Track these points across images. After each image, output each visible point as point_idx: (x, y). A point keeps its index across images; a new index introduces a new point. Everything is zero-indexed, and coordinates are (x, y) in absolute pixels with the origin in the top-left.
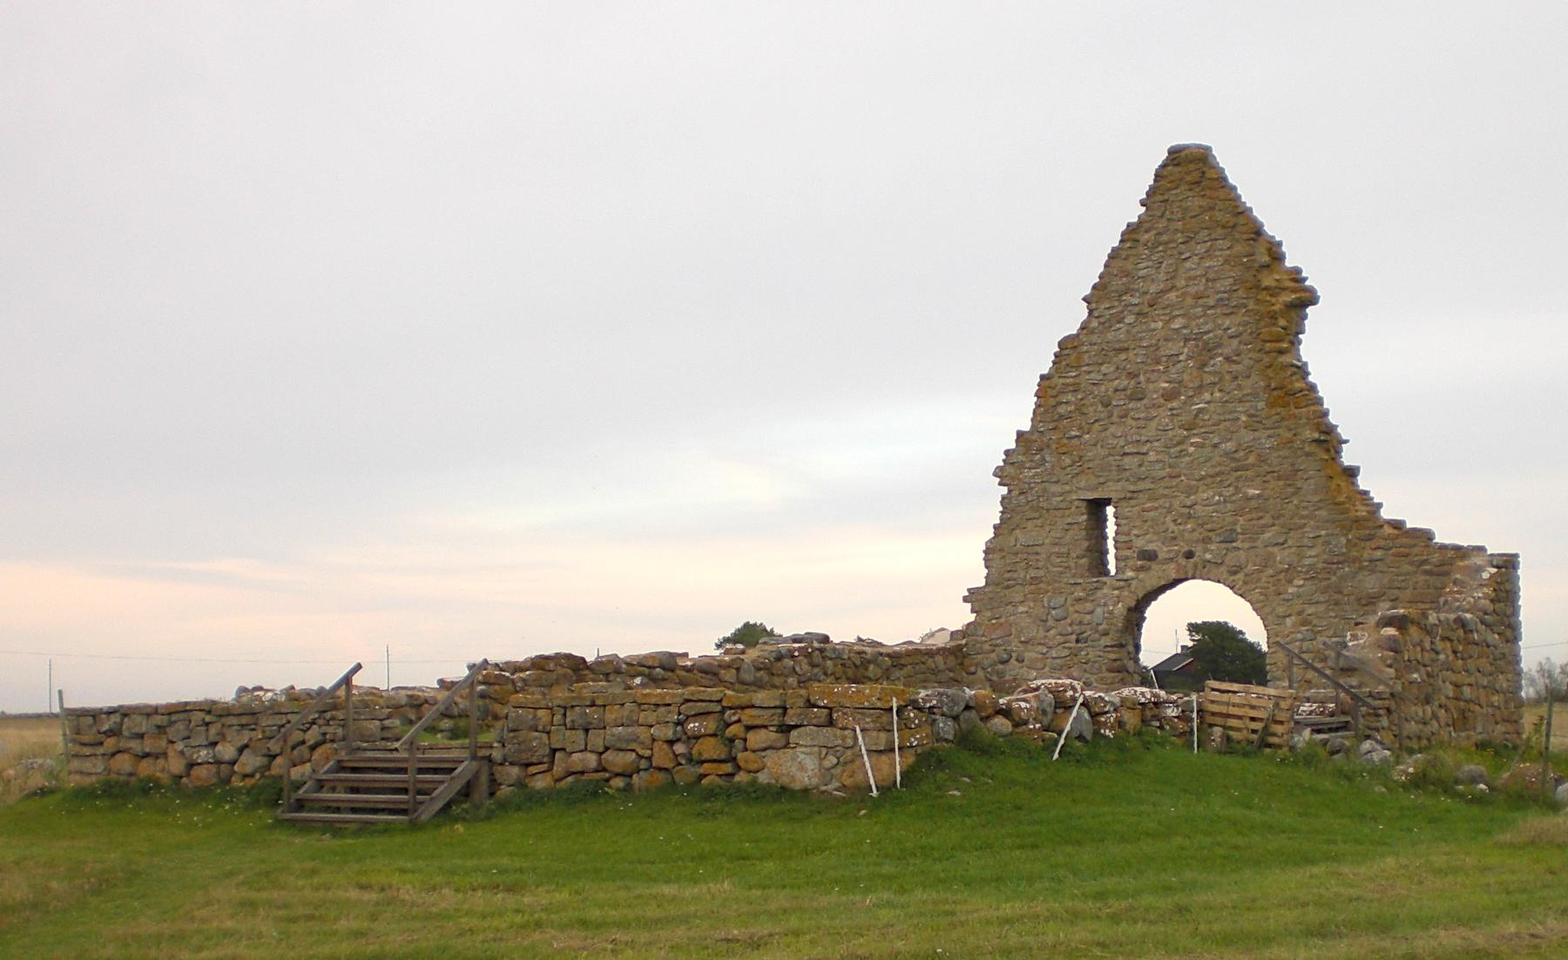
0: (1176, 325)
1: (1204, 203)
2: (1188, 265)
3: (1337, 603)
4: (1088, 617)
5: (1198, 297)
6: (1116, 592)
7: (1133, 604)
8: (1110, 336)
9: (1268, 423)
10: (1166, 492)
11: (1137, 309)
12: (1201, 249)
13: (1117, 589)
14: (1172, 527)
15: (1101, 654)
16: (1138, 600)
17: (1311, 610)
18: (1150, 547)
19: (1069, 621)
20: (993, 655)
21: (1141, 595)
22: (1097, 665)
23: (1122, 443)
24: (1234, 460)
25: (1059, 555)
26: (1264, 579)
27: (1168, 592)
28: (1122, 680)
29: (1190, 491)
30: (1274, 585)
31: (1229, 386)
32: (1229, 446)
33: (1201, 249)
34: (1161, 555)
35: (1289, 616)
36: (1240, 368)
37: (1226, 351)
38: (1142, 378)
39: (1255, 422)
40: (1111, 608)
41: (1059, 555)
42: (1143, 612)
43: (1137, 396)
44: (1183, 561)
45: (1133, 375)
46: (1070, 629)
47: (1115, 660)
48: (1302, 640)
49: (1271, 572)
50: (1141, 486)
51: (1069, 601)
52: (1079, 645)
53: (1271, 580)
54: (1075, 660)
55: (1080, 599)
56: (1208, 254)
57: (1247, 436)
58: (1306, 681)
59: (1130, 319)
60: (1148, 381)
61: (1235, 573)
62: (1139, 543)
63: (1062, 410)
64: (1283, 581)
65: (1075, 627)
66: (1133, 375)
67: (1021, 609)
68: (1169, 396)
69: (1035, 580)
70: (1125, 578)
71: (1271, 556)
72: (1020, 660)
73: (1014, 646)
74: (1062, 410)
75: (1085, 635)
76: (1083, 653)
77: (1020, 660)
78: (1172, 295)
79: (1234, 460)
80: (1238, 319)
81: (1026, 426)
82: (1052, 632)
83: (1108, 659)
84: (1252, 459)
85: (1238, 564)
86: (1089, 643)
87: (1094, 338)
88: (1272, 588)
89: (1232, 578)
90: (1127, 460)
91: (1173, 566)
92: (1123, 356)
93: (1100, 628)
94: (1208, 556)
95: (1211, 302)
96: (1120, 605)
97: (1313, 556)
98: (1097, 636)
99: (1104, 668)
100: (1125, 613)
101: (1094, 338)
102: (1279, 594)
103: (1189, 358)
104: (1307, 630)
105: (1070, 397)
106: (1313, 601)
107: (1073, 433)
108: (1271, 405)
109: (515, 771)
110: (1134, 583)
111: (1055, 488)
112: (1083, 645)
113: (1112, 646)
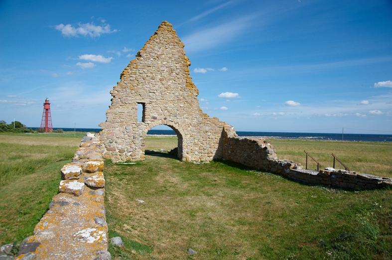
0: (164, 63)
1: (172, 36)
2: (167, 50)
3: (199, 132)
8: (146, 62)
9: (186, 90)
10: (161, 103)
11: (154, 57)
12: (171, 47)
18: (155, 116)
20: (108, 141)
23: (149, 89)
24: (178, 97)
25: (129, 116)
29: (167, 103)
31: (177, 80)
32: (177, 94)
37: (177, 72)
38: (154, 74)
39: (183, 89)
41: (129, 116)
44: (164, 120)
50: (153, 101)
51: (131, 128)
57: (181, 93)
60: (156, 75)
62: (152, 115)
63: (131, 78)
69: (121, 122)
71: (185, 121)
73: (115, 138)
74: (131, 78)
78: (163, 56)
79: (178, 97)
82: (126, 135)
87: (141, 62)
90: (151, 94)
91: (161, 121)
92: (149, 68)
94: (170, 119)
97: (195, 122)
101: (141, 62)
103: (167, 71)
107: (135, 85)
108: (187, 86)
110: (150, 124)
111: (129, 98)
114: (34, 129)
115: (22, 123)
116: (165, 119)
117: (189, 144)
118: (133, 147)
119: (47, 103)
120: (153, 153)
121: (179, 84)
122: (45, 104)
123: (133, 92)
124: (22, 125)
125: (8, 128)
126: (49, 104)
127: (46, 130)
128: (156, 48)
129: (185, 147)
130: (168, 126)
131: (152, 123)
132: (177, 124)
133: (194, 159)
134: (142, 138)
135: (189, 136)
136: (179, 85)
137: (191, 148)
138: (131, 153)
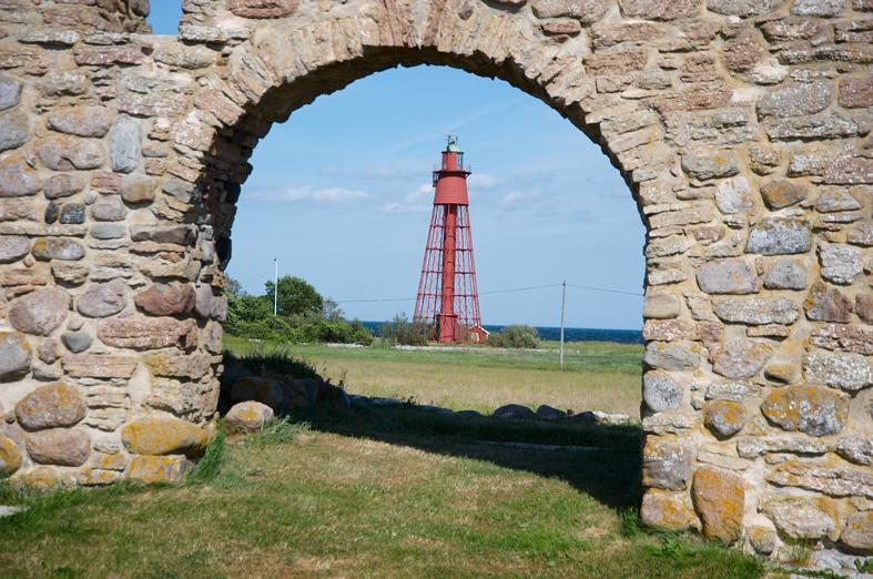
4: (92, 145)
6: (184, 78)
7: (233, 114)
13: (188, 67)
15: (129, 259)
16: (248, 105)
17: (813, 155)
19: (27, 152)
21: (259, 89)
22: (107, 290)
26: (654, 58)
27: (322, 100)
28: (182, 339)
30: (684, 79)
35: (733, 173)
40: (163, 123)
42: (248, 151)
46: (29, 180)
47: (165, 280)
48: (767, 250)
49: (677, 35)
51: (30, 96)
52: (56, 228)
53: (678, 60)
54: (42, 270)
55: (67, 92)
58: (770, 377)
61: (560, 38)
64: (719, 68)
65: (44, 174)
70: (212, 37)
75: (76, 199)
76: (66, 253)
83: (146, 273)
85: (577, 10)
86: (89, 223)
88: (679, 87)
89: (551, 51)
93: (126, 181)
96: (193, 116)
98: (116, 202)
99: (130, 296)
100: (208, 141)
102: (703, 106)
104: (788, 221)
106: (818, 131)
110: (238, 52)
112: (66, 229)
113: (158, 238)
114: (376, 328)
115: (322, 290)
117: (745, 308)
118: (40, 313)
119: (450, 173)
120: (535, 435)
122: (442, 174)
124: (318, 301)
125: (245, 317)
126: (463, 174)
127: (446, 330)
129: (682, 349)
130: (556, 104)
131: (264, 31)
132: (578, 45)
133: (814, 520)
134: (142, 220)
137: (780, 358)
138: (27, 386)
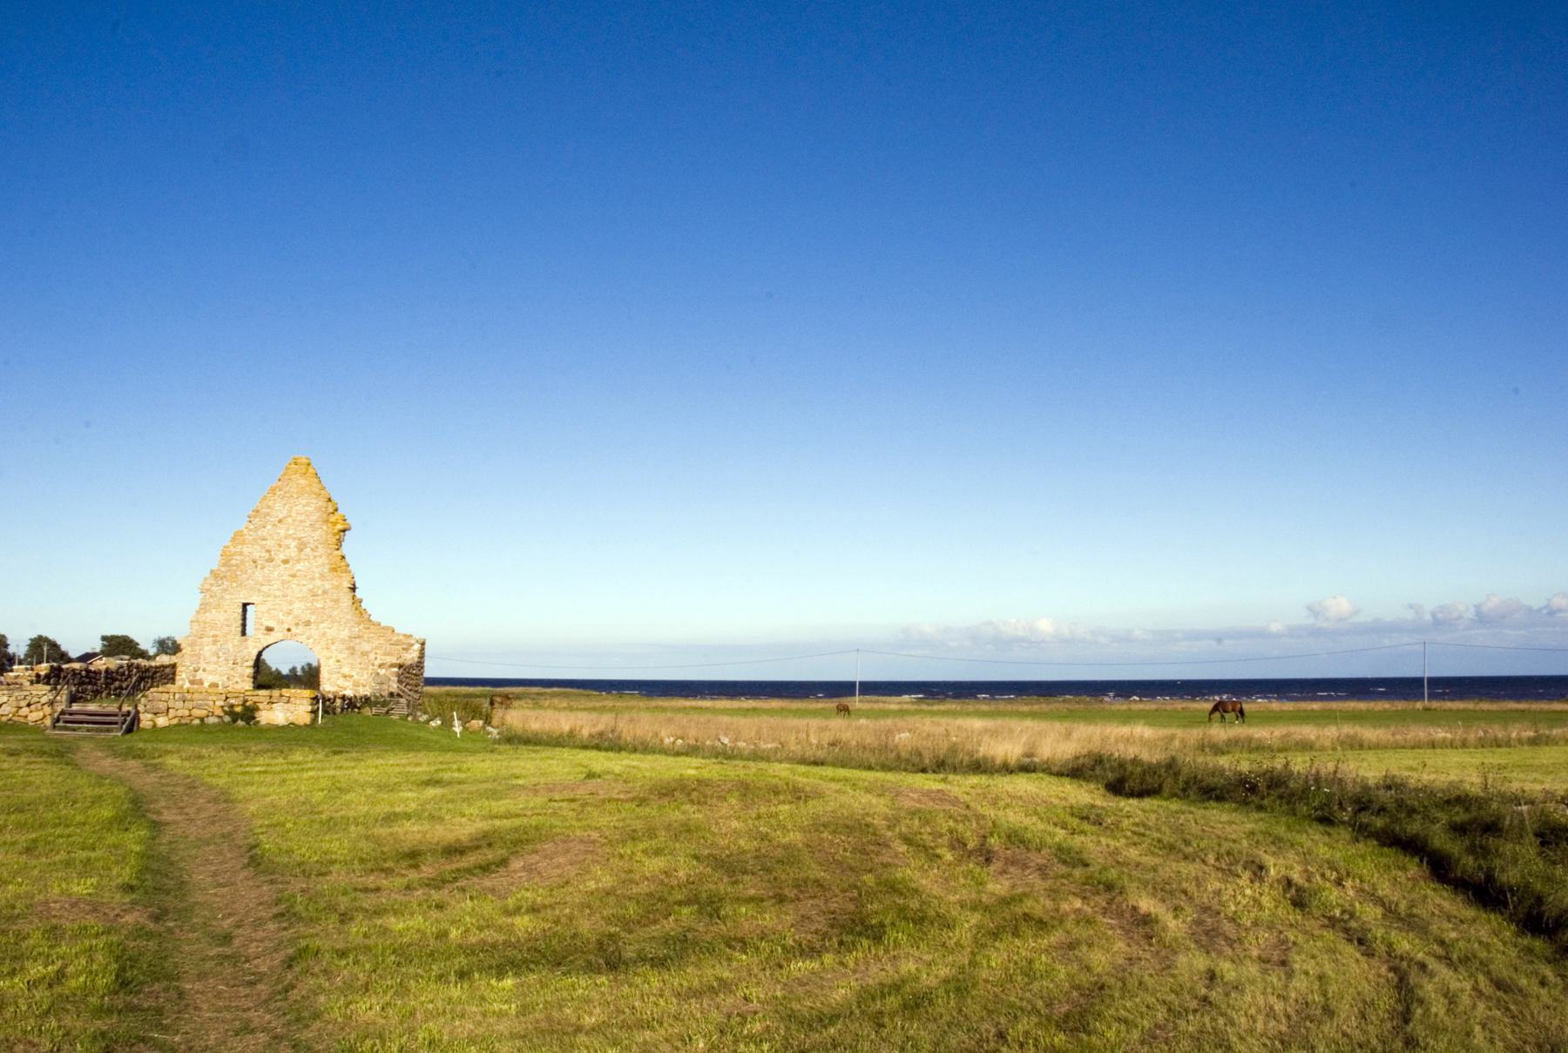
0: (291, 532)
5: (301, 521)
14: (282, 617)
25: (227, 625)
32: (311, 586)
33: (304, 502)
34: (276, 629)
36: (316, 554)
39: (322, 577)
41: (227, 625)
43: (271, 560)
44: (286, 632)
45: (268, 551)
56: (307, 504)
57: (319, 583)
59: (269, 527)
66: (268, 551)
67: (206, 648)
68: (285, 562)
72: (204, 670)
74: (233, 562)
77: (204, 670)
78: (289, 520)
80: (318, 533)
81: (215, 567)
84: (320, 592)
92: (264, 542)
95: (307, 525)
97: (345, 634)
105: (238, 557)
109: (150, 716)
116: (289, 630)
121: (317, 567)
123: (235, 585)
128: (278, 506)
135: (331, 662)
136: (316, 570)
